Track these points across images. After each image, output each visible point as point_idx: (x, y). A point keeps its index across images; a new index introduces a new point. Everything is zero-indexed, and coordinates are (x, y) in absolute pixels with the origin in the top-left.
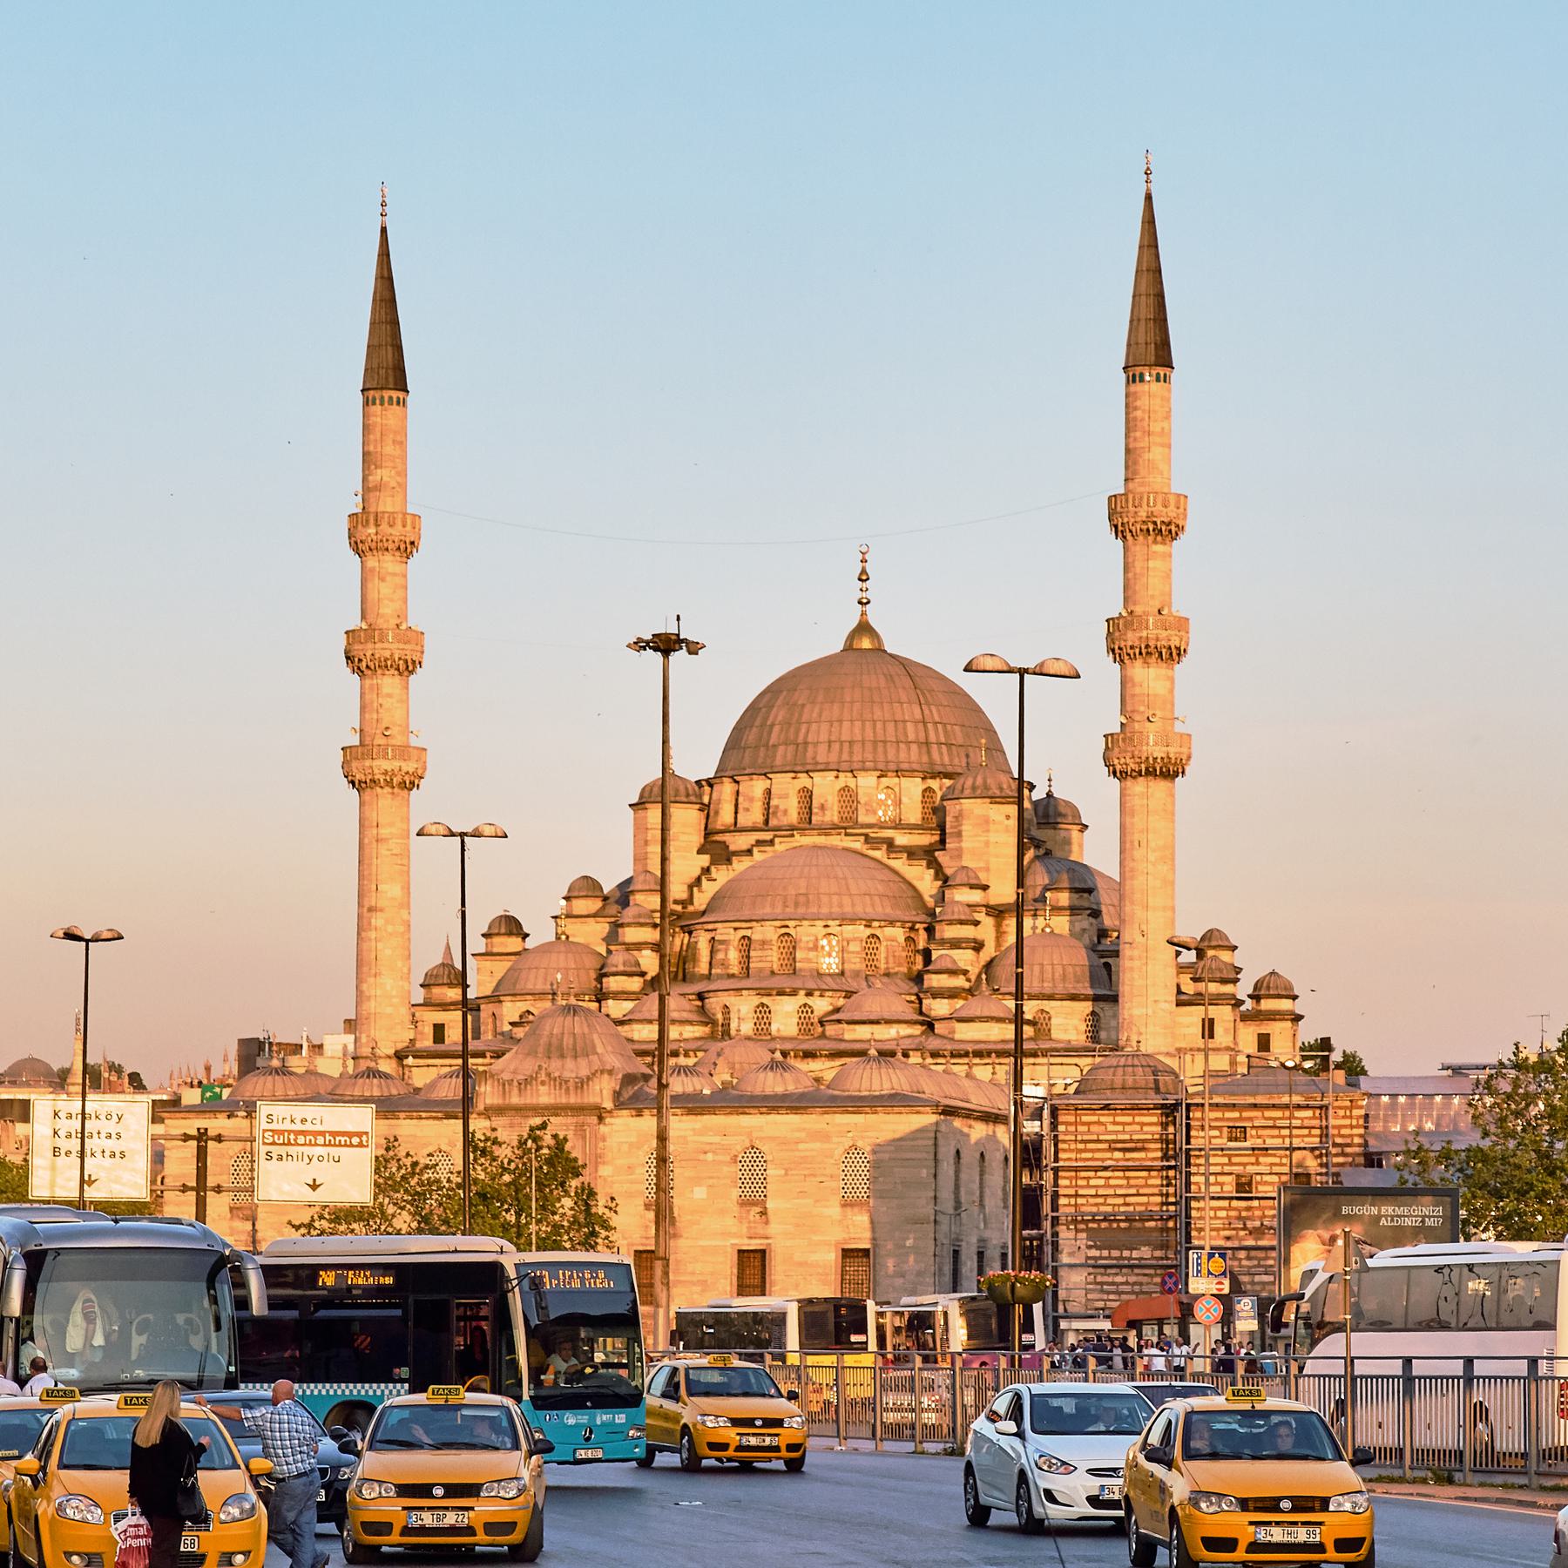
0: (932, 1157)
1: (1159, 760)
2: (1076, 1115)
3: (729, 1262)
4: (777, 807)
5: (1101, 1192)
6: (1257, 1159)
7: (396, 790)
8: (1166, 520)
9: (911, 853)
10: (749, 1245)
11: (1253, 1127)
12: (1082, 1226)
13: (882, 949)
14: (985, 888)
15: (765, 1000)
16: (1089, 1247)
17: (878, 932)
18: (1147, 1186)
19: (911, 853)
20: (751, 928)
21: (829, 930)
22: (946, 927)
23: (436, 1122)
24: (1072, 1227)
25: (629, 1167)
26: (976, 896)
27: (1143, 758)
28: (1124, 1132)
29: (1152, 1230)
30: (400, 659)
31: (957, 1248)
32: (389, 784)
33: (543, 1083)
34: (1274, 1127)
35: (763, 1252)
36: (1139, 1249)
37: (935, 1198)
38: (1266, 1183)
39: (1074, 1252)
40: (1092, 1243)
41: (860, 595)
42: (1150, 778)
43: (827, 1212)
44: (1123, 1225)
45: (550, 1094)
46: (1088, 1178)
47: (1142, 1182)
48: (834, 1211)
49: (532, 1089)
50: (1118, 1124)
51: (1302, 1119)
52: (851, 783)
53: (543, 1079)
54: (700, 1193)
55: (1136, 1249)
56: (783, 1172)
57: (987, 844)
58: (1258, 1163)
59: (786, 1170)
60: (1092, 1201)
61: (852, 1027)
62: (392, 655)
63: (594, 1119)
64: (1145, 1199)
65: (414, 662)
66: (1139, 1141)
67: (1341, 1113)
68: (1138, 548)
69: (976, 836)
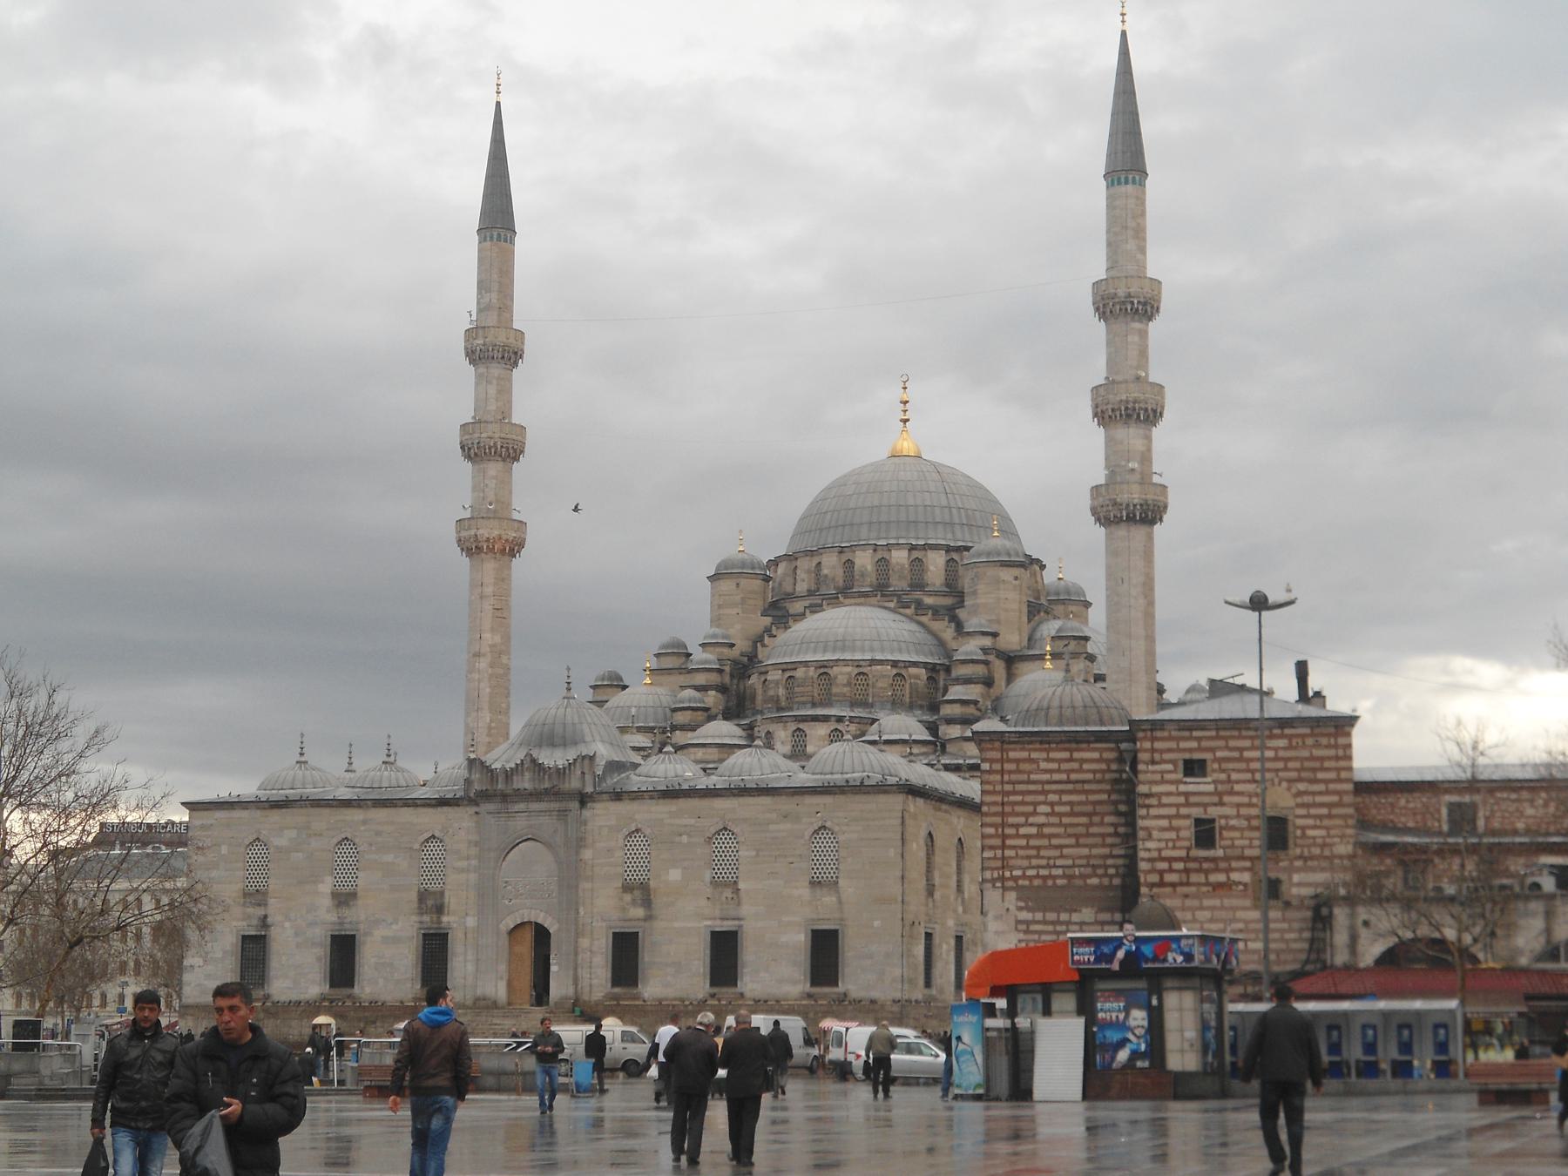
0: (899, 836)
1: (1138, 507)
2: (1002, 751)
4: (826, 576)
5: (1033, 842)
6: (1221, 799)
8: (1142, 300)
9: (936, 612)
11: (1216, 760)
12: (1010, 884)
13: (907, 686)
14: (995, 635)
15: (801, 726)
16: (1020, 909)
17: (903, 672)
18: (1088, 835)
19: (936, 612)
21: (861, 670)
22: (960, 666)
24: (999, 884)
26: (987, 642)
27: (1124, 505)
28: (1059, 771)
29: (1095, 887)
31: (929, 931)
32: (491, 550)
34: (1241, 759)
36: (1080, 911)
37: (903, 877)
38: (1233, 828)
39: (1002, 915)
40: (1022, 904)
44: (1060, 882)
46: (1017, 826)
47: (1082, 830)
48: (804, 892)
50: (1053, 760)
51: (1276, 749)
52: (886, 555)
54: (675, 875)
55: (1075, 911)
56: (754, 853)
58: (1221, 804)
59: (758, 851)
60: (1021, 852)
63: (576, 805)
64: (1085, 851)
65: (515, 451)
66: (1077, 782)
67: (1324, 741)
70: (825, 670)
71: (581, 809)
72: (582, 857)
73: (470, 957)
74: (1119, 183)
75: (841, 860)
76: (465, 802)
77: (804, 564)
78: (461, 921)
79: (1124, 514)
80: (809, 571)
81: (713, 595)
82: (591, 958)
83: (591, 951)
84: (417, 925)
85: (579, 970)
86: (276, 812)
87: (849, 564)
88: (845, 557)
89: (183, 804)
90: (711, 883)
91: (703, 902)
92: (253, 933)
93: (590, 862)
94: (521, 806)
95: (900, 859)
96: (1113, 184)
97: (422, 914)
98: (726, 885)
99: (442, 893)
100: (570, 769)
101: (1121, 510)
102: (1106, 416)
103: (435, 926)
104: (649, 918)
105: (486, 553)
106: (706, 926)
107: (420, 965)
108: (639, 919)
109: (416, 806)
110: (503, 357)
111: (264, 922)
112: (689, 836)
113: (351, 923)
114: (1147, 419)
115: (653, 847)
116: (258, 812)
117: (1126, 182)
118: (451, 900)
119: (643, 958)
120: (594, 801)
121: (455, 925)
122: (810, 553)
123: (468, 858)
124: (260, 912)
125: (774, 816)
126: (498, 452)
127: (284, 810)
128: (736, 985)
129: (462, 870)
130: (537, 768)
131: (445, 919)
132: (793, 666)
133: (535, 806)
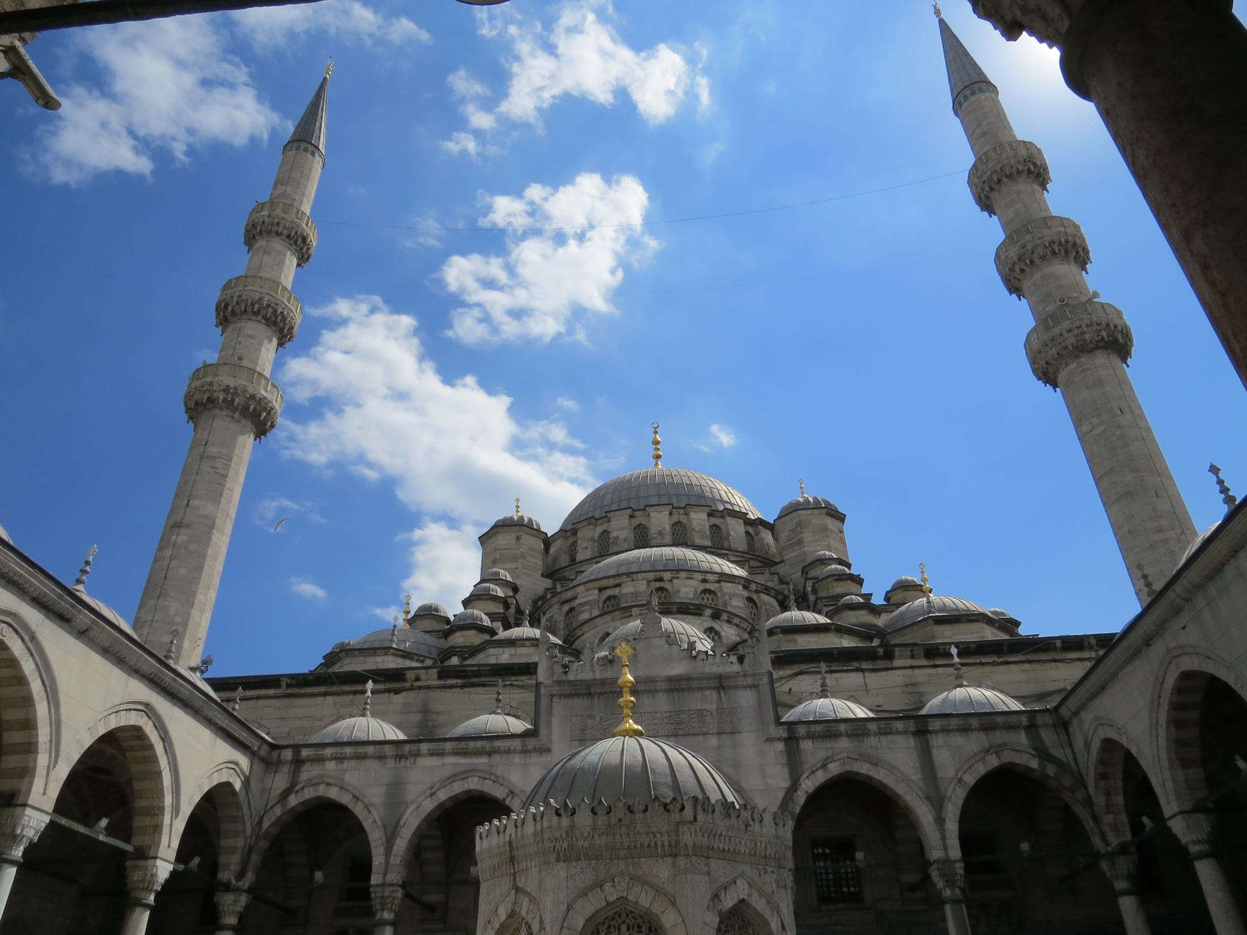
4: (617, 538)
7: (237, 415)
17: (755, 597)
20: (619, 585)
21: (708, 586)
22: (835, 584)
32: (229, 404)
41: (654, 452)
52: (684, 520)
61: (789, 637)
62: (261, 299)
69: (816, 541)
70: (662, 584)
77: (588, 535)
80: (592, 540)
88: (635, 522)
101: (1098, 331)
102: (1035, 256)
105: (221, 409)
122: (592, 521)
126: (263, 312)
132: (617, 581)
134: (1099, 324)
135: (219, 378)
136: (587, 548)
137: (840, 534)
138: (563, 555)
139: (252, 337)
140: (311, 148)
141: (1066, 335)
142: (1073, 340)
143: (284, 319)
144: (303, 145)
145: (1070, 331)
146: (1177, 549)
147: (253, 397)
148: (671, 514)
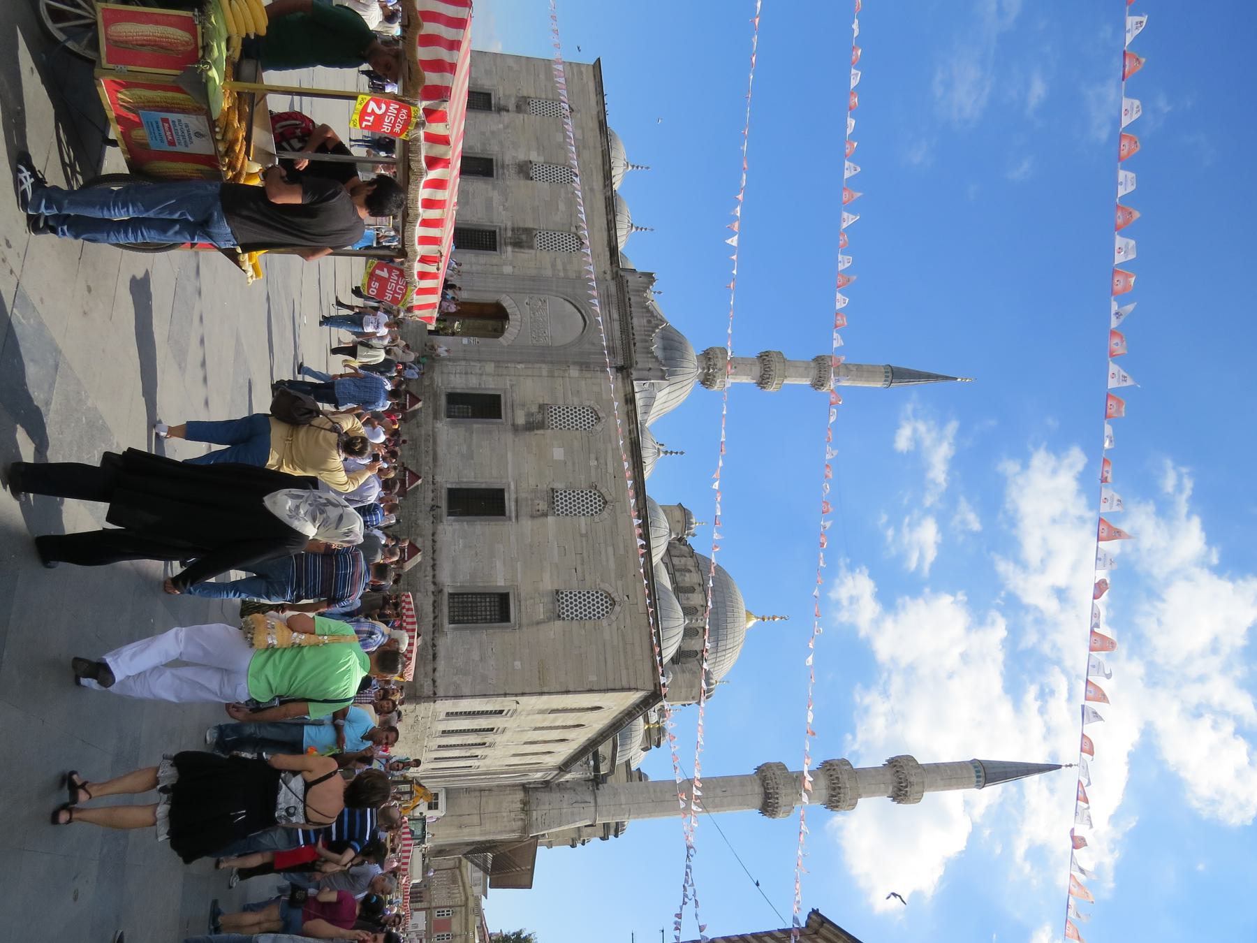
1: (776, 801)
3: (492, 480)
4: (685, 576)
8: (909, 793)
10: (509, 499)
23: (606, 243)
25: (578, 391)
27: (777, 791)
30: (770, 375)
33: (649, 322)
35: (503, 513)
42: (763, 795)
43: (546, 577)
45: (640, 326)
48: (548, 584)
49: (643, 312)
53: (653, 322)
54: (558, 453)
56: (584, 531)
57: (680, 687)
59: (586, 535)
63: (620, 362)
68: (889, 776)
71: (616, 367)
72: (571, 367)
73: (474, 268)
74: (977, 772)
75: (582, 622)
76: (615, 269)
77: (690, 562)
78: (508, 261)
79: (771, 791)
80: (686, 565)
81: (670, 506)
82: (476, 374)
83: (481, 375)
84: (503, 226)
85: (463, 363)
86: (596, 126)
87: (692, 590)
88: (696, 587)
89: (599, 59)
90: (553, 490)
91: (532, 482)
92: (493, 102)
93: (567, 375)
94: (615, 316)
95: (588, 687)
96: (971, 763)
97: (513, 230)
98: (552, 502)
99: (531, 247)
100: (651, 357)
101: (773, 788)
102: (832, 773)
103: (503, 241)
104: (516, 429)
105: (706, 364)
106: (509, 485)
107: (467, 227)
108: (514, 420)
109: (609, 230)
110: (820, 377)
111: (502, 109)
112: (597, 467)
113: (503, 174)
114: (831, 801)
115: (584, 432)
116: (596, 113)
117: (978, 777)
118: (525, 255)
119: (477, 423)
120: (623, 379)
121: (504, 257)
122: (697, 566)
123: (565, 269)
124: (512, 107)
125: (622, 551)
126: (766, 373)
127: (598, 130)
128: (450, 514)
129: (554, 265)
130: (651, 329)
131: (509, 249)
133: (616, 326)
134: (777, 788)
135: (720, 361)
136: (680, 562)
137: (691, 697)
138: (679, 551)
139: (751, 370)
140: (890, 379)
141: (772, 772)
142: (769, 776)
143: (766, 383)
144: (890, 375)
145: (774, 774)
146: (644, 796)
147: (714, 377)
148: (702, 606)
